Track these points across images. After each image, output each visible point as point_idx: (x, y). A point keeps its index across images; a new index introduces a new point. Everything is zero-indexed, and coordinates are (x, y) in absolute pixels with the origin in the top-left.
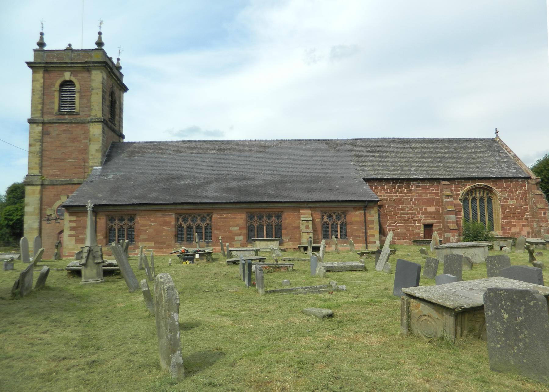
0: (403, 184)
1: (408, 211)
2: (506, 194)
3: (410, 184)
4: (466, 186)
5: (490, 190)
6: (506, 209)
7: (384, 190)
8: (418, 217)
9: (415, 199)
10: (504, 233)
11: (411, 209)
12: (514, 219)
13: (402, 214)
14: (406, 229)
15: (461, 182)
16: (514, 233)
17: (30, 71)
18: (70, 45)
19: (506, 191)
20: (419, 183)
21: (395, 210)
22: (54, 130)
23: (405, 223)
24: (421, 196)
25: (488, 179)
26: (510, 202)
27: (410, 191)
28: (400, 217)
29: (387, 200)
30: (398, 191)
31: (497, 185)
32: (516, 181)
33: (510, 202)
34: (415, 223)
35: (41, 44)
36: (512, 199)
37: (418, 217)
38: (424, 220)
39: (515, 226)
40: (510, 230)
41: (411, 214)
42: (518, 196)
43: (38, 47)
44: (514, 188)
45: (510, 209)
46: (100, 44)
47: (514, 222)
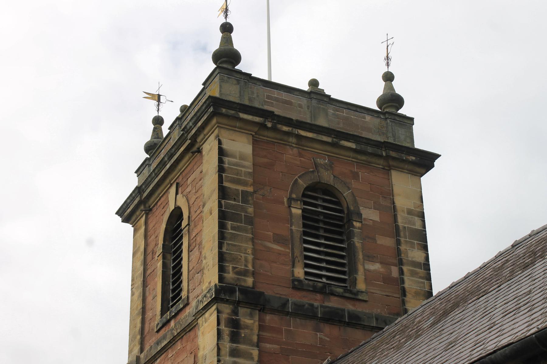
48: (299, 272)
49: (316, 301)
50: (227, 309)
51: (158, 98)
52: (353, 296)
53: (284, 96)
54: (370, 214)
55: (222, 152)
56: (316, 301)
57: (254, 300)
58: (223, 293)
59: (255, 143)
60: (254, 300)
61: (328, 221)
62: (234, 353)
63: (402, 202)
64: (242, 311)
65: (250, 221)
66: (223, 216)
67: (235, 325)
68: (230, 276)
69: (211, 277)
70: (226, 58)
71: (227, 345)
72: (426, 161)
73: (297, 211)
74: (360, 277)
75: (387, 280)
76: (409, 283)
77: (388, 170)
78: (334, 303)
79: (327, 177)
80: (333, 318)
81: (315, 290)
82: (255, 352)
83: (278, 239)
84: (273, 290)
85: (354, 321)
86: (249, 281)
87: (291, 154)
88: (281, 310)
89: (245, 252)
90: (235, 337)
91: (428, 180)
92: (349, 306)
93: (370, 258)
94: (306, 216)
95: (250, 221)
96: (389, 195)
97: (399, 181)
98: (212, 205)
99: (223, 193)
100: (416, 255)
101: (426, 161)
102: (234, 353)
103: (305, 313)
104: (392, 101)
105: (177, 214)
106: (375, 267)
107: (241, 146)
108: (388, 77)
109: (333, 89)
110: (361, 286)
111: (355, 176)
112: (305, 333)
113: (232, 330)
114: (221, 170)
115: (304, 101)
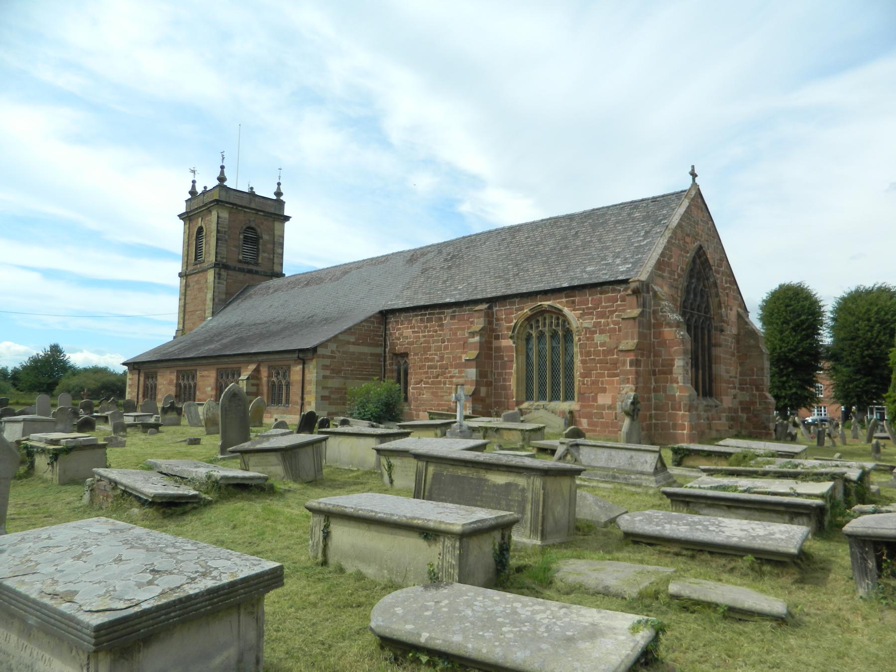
0: (433, 314)
1: (438, 361)
2: (588, 323)
3: (444, 313)
4: (523, 309)
5: (559, 313)
6: (588, 354)
7: (411, 328)
8: (449, 372)
9: (449, 340)
10: (582, 406)
11: (442, 358)
12: (602, 375)
13: (430, 367)
14: (433, 393)
15: (513, 304)
16: (603, 407)
17: (182, 222)
18: (205, 188)
19: (591, 314)
20: (454, 312)
21: (421, 360)
22: (193, 279)
23: (433, 383)
24: (455, 334)
25: (546, 293)
26: (598, 338)
27: (441, 325)
28: (427, 373)
29: (412, 343)
30: (426, 327)
31: (573, 302)
32: (614, 291)
34: (445, 384)
35: (193, 192)
38: (458, 377)
39: (604, 390)
40: (595, 399)
41: (441, 367)
42: (615, 323)
43: (190, 196)
44: (607, 307)
45: (597, 353)
46: (222, 179)
47: (602, 383)
48: (241, 257)
49: (245, 266)
50: (217, 270)
51: (194, 172)
52: (257, 264)
53: (241, 194)
54: (266, 237)
55: (218, 217)
56: (245, 266)
57: (226, 267)
58: (216, 265)
59: (230, 213)
60: (226, 267)
62: (219, 283)
63: (277, 233)
64: (222, 270)
65: (226, 241)
66: (217, 239)
67: (219, 274)
68: (219, 259)
69: (212, 259)
70: (222, 179)
71: (217, 281)
72: (287, 218)
73: (242, 237)
74: (260, 258)
75: (269, 259)
76: (276, 260)
77: (274, 221)
78: (250, 267)
79: (253, 225)
80: (250, 271)
81: (245, 263)
83: (235, 246)
84: (230, 263)
85: (257, 273)
86: (225, 261)
87: (241, 217)
88: (234, 269)
89: (223, 250)
90: (219, 278)
91: (287, 224)
92: (254, 268)
93: (264, 252)
94: (245, 237)
95: (226, 241)
96: (273, 230)
97: (277, 225)
98: (214, 233)
99: (218, 231)
100: (279, 251)
101: (287, 218)
102: (219, 283)
103: (241, 270)
104: (279, 194)
105: (200, 230)
106: (266, 255)
107: (225, 215)
108: (279, 184)
109: (258, 192)
110: (260, 261)
111: (262, 224)
112: (241, 276)
113: (218, 276)
114: (218, 223)
115: (248, 196)
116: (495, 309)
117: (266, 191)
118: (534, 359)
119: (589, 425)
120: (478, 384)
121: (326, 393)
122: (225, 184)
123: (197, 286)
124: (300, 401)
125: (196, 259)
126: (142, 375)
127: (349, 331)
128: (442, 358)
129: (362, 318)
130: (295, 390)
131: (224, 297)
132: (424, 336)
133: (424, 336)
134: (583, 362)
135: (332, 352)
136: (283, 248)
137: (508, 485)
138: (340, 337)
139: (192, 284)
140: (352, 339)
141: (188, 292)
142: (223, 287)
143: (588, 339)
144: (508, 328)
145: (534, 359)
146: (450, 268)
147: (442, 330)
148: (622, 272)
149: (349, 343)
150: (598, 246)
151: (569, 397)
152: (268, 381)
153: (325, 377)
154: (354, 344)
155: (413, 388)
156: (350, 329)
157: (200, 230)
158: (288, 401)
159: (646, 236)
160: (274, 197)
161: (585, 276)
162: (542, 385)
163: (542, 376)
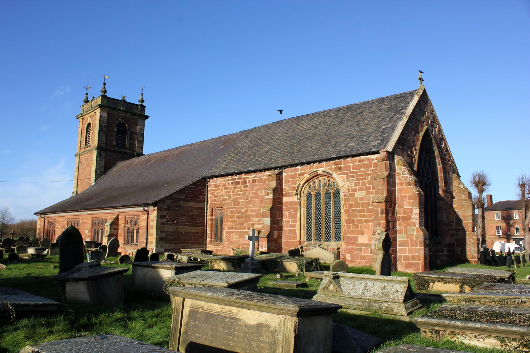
1: (243, 213)
4: (303, 174)
12: (361, 221)
13: (238, 217)
16: (361, 245)
19: (353, 176)
21: (232, 212)
24: (256, 193)
26: (358, 194)
30: (235, 188)
31: (340, 168)
33: (358, 194)
36: (361, 190)
37: (252, 221)
39: (362, 233)
40: (356, 239)
42: (370, 183)
44: (363, 171)
45: (357, 205)
47: (361, 228)
61: (122, 131)
62: (99, 160)
72: (147, 117)
82: (104, 160)
91: (146, 121)
94: (118, 129)
97: (139, 121)
98: (97, 127)
101: (147, 117)
105: (89, 125)
109: (127, 100)
116: (284, 175)
117: (134, 99)
118: (313, 211)
119: (351, 257)
120: (271, 228)
121: (164, 235)
122: (106, 94)
123: (85, 163)
124: (145, 241)
125: (86, 145)
126: (46, 221)
127: (181, 191)
128: (246, 211)
129: (190, 182)
130: (142, 232)
131: (103, 169)
132: (234, 195)
133: (234, 195)
134: (347, 211)
135: (168, 206)
136: (143, 137)
137: (260, 326)
138: (175, 196)
139: (83, 161)
140: (183, 197)
141: (80, 167)
142: (103, 163)
143: (351, 195)
144: (294, 188)
145: (313, 211)
146: (253, 147)
147: (246, 190)
148: (375, 146)
149: (180, 199)
150: (357, 128)
151: (338, 238)
152: (125, 227)
153: (162, 224)
154: (183, 200)
155: (227, 232)
156: (181, 190)
157: (89, 125)
158: (137, 241)
159: (389, 121)
160: (139, 103)
161: (348, 149)
162: (318, 229)
163: (318, 223)
